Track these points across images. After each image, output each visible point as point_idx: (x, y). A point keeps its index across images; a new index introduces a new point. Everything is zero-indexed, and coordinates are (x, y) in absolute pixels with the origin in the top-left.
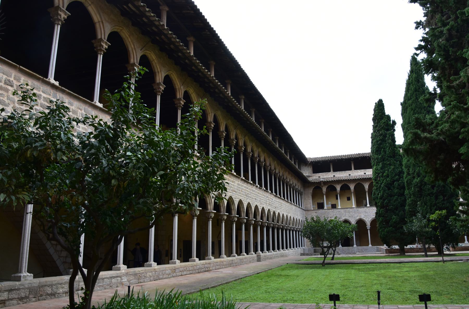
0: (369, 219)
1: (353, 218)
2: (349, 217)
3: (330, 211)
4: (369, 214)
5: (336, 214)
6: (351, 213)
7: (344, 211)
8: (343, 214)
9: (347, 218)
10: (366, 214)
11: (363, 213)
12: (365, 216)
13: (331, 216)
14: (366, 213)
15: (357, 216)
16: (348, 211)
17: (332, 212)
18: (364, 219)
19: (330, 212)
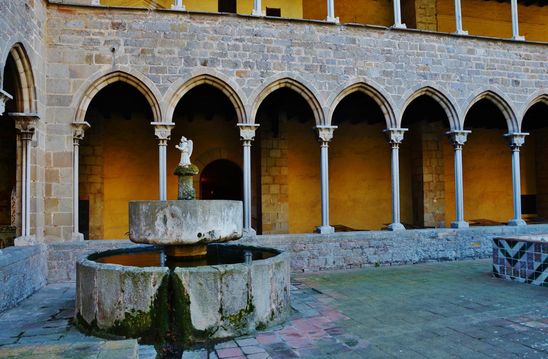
0: (401, 91)
1: (328, 78)
2: (307, 68)
3: (207, 23)
4: (401, 67)
5: (236, 48)
6: (318, 51)
7: (281, 36)
8: (279, 51)
9: (296, 75)
10: (391, 67)
11: (376, 58)
12: (385, 73)
13: (208, 57)
14: (388, 59)
15: (347, 71)
16: (303, 36)
17: (216, 31)
18: (381, 88)
19: (205, 30)
